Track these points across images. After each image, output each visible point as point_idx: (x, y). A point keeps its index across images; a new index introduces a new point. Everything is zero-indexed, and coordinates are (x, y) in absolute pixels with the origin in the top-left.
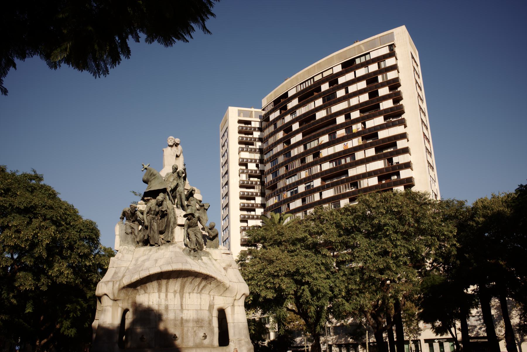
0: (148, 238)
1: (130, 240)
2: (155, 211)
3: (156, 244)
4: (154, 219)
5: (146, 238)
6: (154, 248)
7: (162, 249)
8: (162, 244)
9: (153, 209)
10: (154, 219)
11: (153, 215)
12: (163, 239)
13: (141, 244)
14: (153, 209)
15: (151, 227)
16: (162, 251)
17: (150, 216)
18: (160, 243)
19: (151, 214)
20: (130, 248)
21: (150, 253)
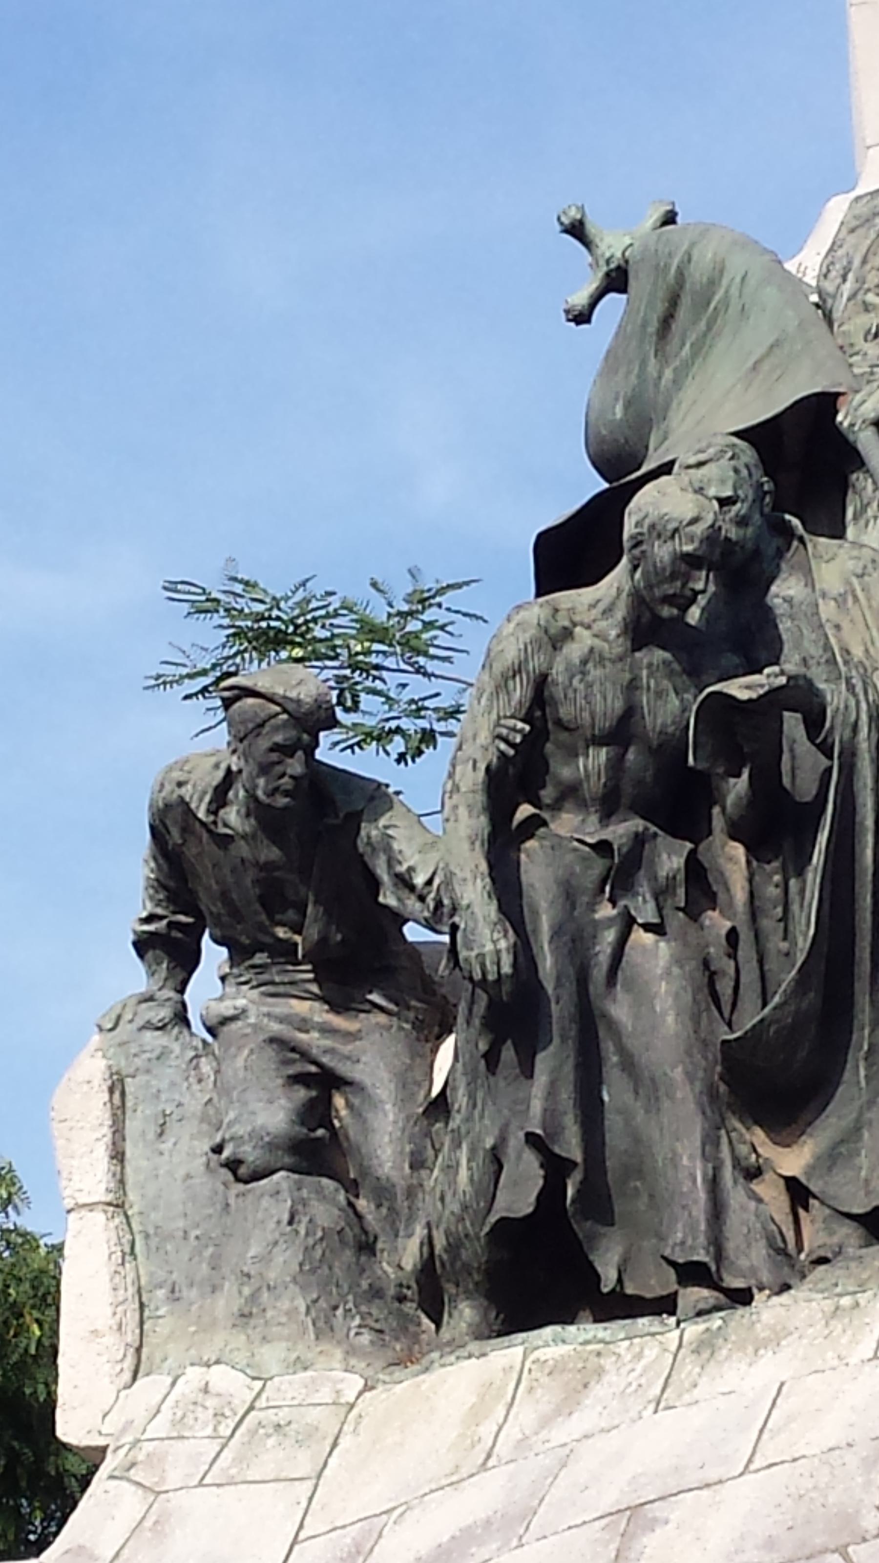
0: (551, 1192)
1: (285, 1261)
2: (621, 733)
3: (712, 1283)
4: (621, 870)
5: (519, 1195)
6: (638, 1351)
7: (776, 1338)
8: (790, 1266)
9: (593, 700)
10: (621, 870)
11: (609, 806)
12: (798, 1193)
13: (464, 1313)
14: (593, 700)
15: (589, 1026)
16: (769, 1369)
17: (566, 824)
18: (748, 1259)
19: (570, 794)
20: (287, 1388)
21: (585, 1418)
